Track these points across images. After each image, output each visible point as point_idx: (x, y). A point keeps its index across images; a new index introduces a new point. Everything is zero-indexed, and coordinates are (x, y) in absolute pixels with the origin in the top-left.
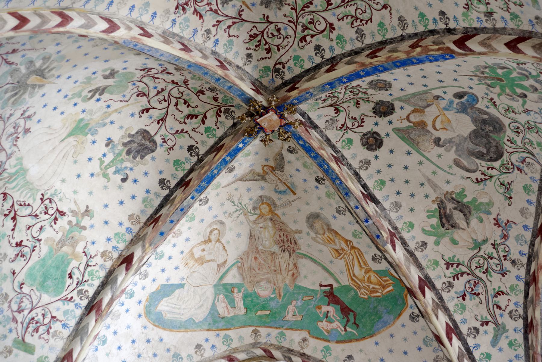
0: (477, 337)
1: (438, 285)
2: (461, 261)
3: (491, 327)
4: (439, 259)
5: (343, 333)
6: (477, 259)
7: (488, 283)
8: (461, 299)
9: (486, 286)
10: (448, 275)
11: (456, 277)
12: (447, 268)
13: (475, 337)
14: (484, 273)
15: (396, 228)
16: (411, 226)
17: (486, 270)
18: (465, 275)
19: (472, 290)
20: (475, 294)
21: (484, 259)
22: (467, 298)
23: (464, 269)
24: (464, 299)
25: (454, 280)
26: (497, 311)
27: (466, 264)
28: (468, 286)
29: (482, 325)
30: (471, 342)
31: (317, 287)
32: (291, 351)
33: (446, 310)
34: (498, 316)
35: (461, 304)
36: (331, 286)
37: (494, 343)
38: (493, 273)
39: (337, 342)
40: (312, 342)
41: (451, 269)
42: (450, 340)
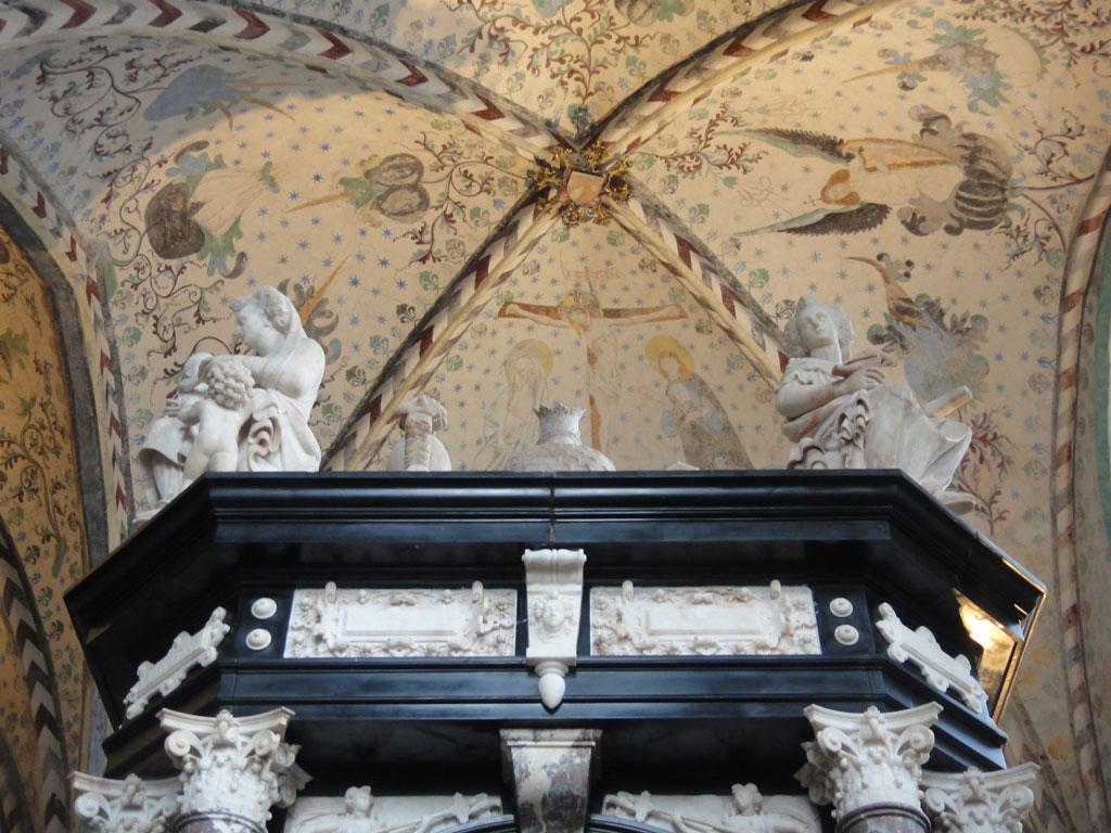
2: (12, 436)
3: (52, 545)
6: (29, 431)
7: (45, 471)
8: (17, 499)
9: (43, 476)
13: (34, 563)
14: (40, 454)
17: (42, 449)
18: (20, 459)
19: (30, 485)
20: (33, 490)
21: (37, 430)
22: (25, 498)
23: (18, 450)
24: (21, 501)
25: (6, 468)
26: (58, 516)
27: (18, 440)
28: (24, 477)
29: (43, 542)
30: (30, 571)
34: (59, 525)
35: (18, 508)
38: (49, 454)
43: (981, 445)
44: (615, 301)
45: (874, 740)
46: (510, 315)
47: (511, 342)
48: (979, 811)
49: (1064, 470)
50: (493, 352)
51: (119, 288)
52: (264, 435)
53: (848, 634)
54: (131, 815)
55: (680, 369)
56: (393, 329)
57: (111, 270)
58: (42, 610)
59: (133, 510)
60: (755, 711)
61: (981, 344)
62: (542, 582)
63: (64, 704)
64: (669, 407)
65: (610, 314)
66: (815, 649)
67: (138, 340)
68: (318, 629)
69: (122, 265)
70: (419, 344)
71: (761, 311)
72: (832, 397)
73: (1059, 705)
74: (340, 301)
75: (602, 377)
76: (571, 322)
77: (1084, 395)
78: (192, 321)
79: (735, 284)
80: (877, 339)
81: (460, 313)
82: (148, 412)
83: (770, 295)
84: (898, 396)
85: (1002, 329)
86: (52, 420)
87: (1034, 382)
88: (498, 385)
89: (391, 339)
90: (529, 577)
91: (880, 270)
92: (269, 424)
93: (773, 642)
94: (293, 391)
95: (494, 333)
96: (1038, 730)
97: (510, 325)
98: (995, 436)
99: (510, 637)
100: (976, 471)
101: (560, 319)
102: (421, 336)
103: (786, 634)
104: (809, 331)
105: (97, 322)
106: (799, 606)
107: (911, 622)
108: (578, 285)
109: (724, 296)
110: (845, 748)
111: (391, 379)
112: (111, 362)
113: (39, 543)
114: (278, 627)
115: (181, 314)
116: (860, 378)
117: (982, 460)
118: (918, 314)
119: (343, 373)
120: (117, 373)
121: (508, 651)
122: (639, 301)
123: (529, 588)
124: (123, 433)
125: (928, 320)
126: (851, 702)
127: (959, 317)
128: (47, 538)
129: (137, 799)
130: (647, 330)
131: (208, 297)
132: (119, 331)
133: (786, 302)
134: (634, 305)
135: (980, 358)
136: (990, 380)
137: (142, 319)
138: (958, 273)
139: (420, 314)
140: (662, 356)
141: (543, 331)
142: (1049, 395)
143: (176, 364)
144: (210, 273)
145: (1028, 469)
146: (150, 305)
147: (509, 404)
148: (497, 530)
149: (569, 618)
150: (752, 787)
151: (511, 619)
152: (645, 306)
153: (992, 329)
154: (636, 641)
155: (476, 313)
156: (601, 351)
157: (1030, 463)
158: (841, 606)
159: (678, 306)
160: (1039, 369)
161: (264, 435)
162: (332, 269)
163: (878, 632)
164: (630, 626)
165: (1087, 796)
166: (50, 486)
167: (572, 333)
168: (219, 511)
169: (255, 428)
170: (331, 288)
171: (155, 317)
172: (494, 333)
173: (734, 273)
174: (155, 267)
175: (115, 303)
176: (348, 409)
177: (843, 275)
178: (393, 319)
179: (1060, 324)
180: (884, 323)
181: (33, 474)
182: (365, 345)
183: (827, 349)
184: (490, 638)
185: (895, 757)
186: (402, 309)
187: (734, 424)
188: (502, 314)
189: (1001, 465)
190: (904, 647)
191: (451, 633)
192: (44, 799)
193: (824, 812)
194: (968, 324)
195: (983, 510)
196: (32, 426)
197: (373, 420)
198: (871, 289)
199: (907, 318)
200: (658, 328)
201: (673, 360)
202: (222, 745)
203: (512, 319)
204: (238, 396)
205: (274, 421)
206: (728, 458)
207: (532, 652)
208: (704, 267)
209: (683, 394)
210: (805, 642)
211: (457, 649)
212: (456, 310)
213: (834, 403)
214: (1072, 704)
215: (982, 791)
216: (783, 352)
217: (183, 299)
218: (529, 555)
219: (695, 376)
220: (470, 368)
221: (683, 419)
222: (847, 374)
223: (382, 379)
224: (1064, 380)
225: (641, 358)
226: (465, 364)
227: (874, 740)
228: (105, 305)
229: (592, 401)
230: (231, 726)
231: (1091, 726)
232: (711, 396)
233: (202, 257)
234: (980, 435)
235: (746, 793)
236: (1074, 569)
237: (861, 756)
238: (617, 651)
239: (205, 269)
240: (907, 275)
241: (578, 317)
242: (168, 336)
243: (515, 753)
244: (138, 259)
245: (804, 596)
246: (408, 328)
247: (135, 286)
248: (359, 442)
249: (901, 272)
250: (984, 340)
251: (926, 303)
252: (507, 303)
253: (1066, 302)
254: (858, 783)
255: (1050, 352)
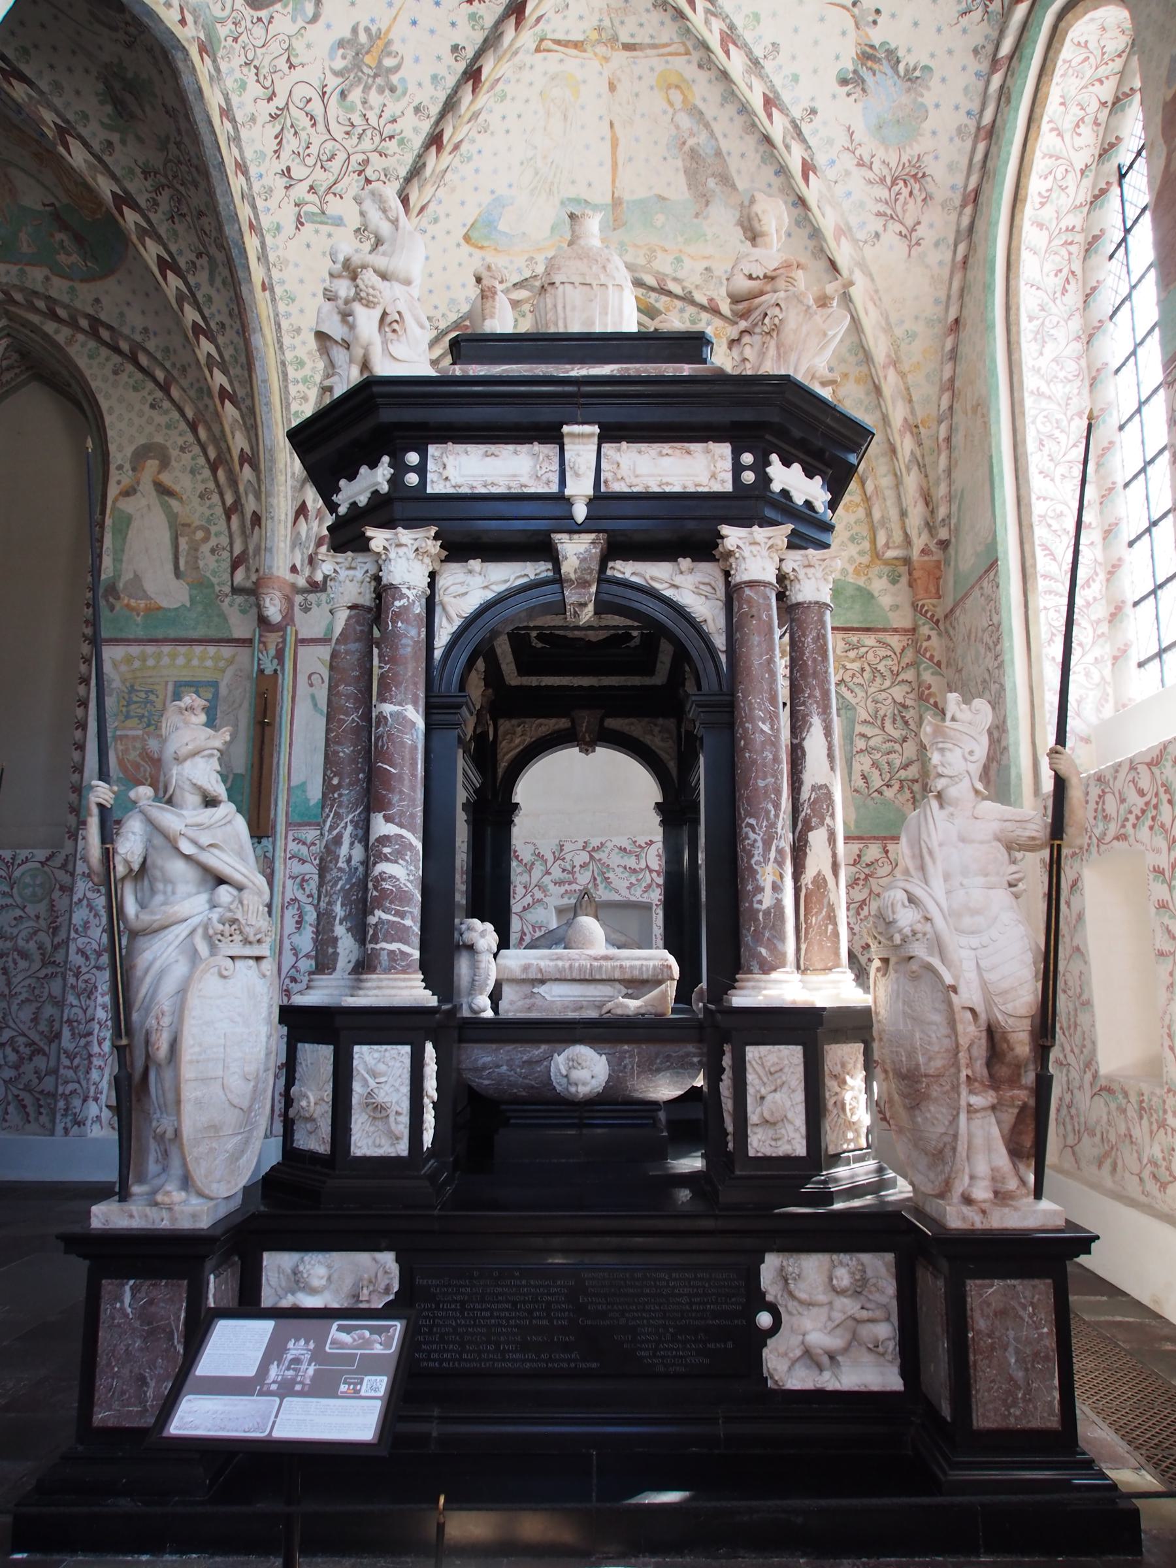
0: (197, 273)
1: (143, 203)
3: (204, 261)
4: (133, 165)
5: (85, 269)
10: (150, 189)
11: (158, 189)
12: (146, 179)
15: (67, 121)
16: (85, 117)
22: (176, 220)
23: (163, 180)
30: (192, 280)
31: (41, 208)
32: (35, 293)
33: (159, 239)
36: (52, 205)
37: (212, 282)
39: (82, 281)
40: (56, 281)
41: (150, 180)
42: (165, 278)
43: (912, 181)
44: (632, 36)
45: (755, 543)
46: (545, 50)
47: (545, 73)
48: (810, 571)
49: (968, 210)
50: (531, 84)
51: (223, 43)
52: (395, 326)
53: (749, 477)
54: (351, 572)
55: (683, 102)
56: (449, 67)
57: (215, 29)
58: (207, 313)
59: (262, 235)
60: (691, 525)
61: (925, 92)
62: (573, 443)
63: (236, 384)
64: (674, 132)
65: (628, 47)
66: (728, 487)
67: (244, 89)
68: (446, 473)
69: (222, 21)
70: (471, 82)
71: (751, 53)
72: (762, 293)
73: (933, 391)
74: (403, 41)
75: (620, 104)
76: (595, 54)
77: (994, 149)
78: (285, 67)
79: (732, 27)
80: (844, 82)
81: (505, 52)
82: (262, 152)
83: (760, 37)
84: (801, 302)
85: (943, 80)
86: (187, 158)
87: (960, 131)
88: (536, 113)
89: (448, 77)
90: (566, 440)
91: (853, 16)
92: (397, 317)
93: (705, 481)
94: (408, 282)
95: (532, 67)
96: (916, 406)
97: (545, 59)
98: (924, 175)
99: (555, 478)
100: (905, 203)
101: (585, 51)
102: (473, 75)
103: (713, 476)
104: (756, 224)
105: (211, 77)
106: (722, 457)
107: (787, 463)
108: (601, 20)
109: (722, 40)
110: (738, 547)
111: (450, 114)
112: (227, 112)
113: (194, 259)
114: (421, 470)
115: (275, 62)
116: (781, 283)
117: (911, 194)
118: (880, 60)
119: (411, 110)
120: (233, 121)
121: (554, 488)
122: (652, 37)
123: (566, 447)
124: (245, 173)
125: (886, 67)
126: (744, 521)
127: (911, 66)
128: (199, 255)
129: (353, 565)
130: (658, 63)
131: (295, 43)
132: (229, 83)
133: (773, 44)
134: (647, 40)
135: (923, 105)
136: (927, 126)
137: (245, 70)
138: (916, 24)
139: (470, 53)
140: (669, 87)
141: (572, 62)
142: (969, 144)
143: (277, 108)
144: (294, 20)
145: (943, 205)
146: (250, 57)
147: (545, 129)
148: (545, 414)
149: (589, 468)
150: (689, 560)
151: (556, 467)
152: (656, 41)
153: (934, 82)
154: (628, 480)
155: (516, 53)
156: (619, 80)
157: (946, 200)
158: (747, 458)
159: (684, 44)
160: (967, 121)
161: (395, 326)
162: (394, 11)
163: (766, 474)
164: (624, 471)
165: (939, 454)
166: (194, 213)
167: (595, 64)
168: (379, 400)
169: (389, 319)
170: (394, 29)
171: (255, 67)
172: (532, 67)
173: (731, 16)
174: (249, 19)
175: (222, 58)
176: (417, 142)
177: (822, 19)
178: (449, 58)
179: (988, 83)
180: (851, 68)
181: (179, 201)
182: (427, 82)
183: (766, 238)
184: (544, 478)
185: (765, 553)
186: (455, 49)
187: (724, 151)
188: (538, 50)
189: (924, 200)
190: (781, 482)
191: (522, 476)
192: (236, 454)
193: (727, 574)
194: (917, 73)
195: (905, 236)
196: (170, 161)
197: (439, 151)
198: (844, 33)
199: (869, 64)
200: (667, 62)
201: (678, 92)
202: (399, 545)
203: (545, 54)
204: (376, 300)
205: (399, 313)
206: (718, 179)
207: (568, 492)
208: (707, 11)
209: (685, 121)
210: (723, 481)
211: (526, 486)
212: (500, 51)
213: (763, 298)
214: (942, 391)
215: (814, 561)
216: (767, 92)
217: (275, 48)
218: (566, 429)
219: (695, 107)
220: (513, 99)
221: (684, 143)
222: (773, 278)
223: (442, 115)
224: (982, 134)
225: (652, 88)
226: (509, 97)
227: (755, 543)
228: (214, 61)
229: (612, 125)
230: (405, 535)
231: (951, 408)
232: (707, 126)
233: (286, 6)
234: (913, 173)
235: (685, 563)
236: (962, 290)
237: (746, 554)
238: (618, 487)
239: (289, 17)
240: (875, 22)
241: (601, 50)
242: (268, 84)
243: (560, 547)
244: (234, 14)
245: (724, 450)
246: (461, 67)
247: (235, 40)
248: (428, 171)
249: (871, 19)
250: (928, 88)
251: (887, 51)
252: (542, 40)
253: (995, 63)
254: (743, 566)
255: (975, 106)
